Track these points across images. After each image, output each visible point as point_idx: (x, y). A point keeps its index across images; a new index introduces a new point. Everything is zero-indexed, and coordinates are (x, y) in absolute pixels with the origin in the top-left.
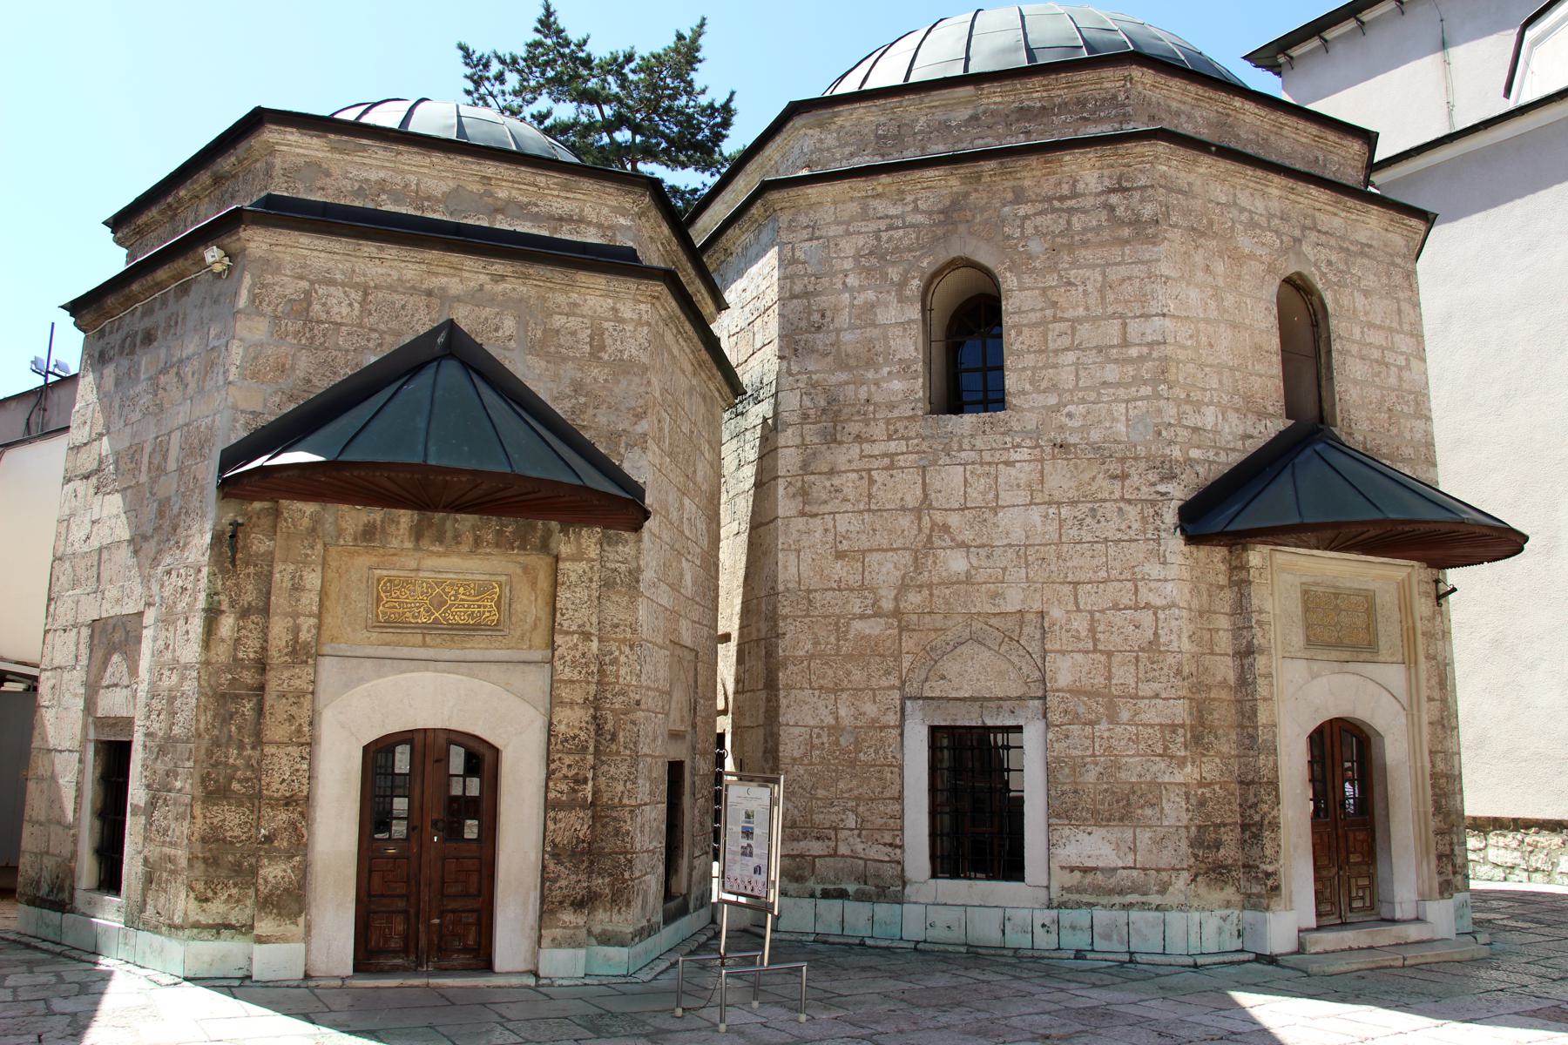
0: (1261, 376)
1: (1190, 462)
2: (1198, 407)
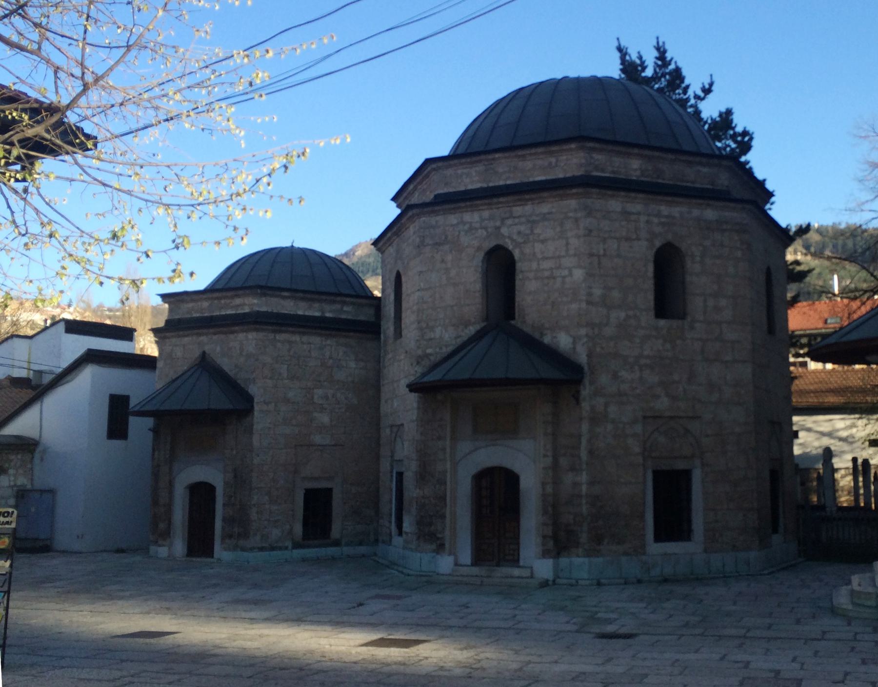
0: (468, 305)
1: (427, 356)
2: (432, 329)
